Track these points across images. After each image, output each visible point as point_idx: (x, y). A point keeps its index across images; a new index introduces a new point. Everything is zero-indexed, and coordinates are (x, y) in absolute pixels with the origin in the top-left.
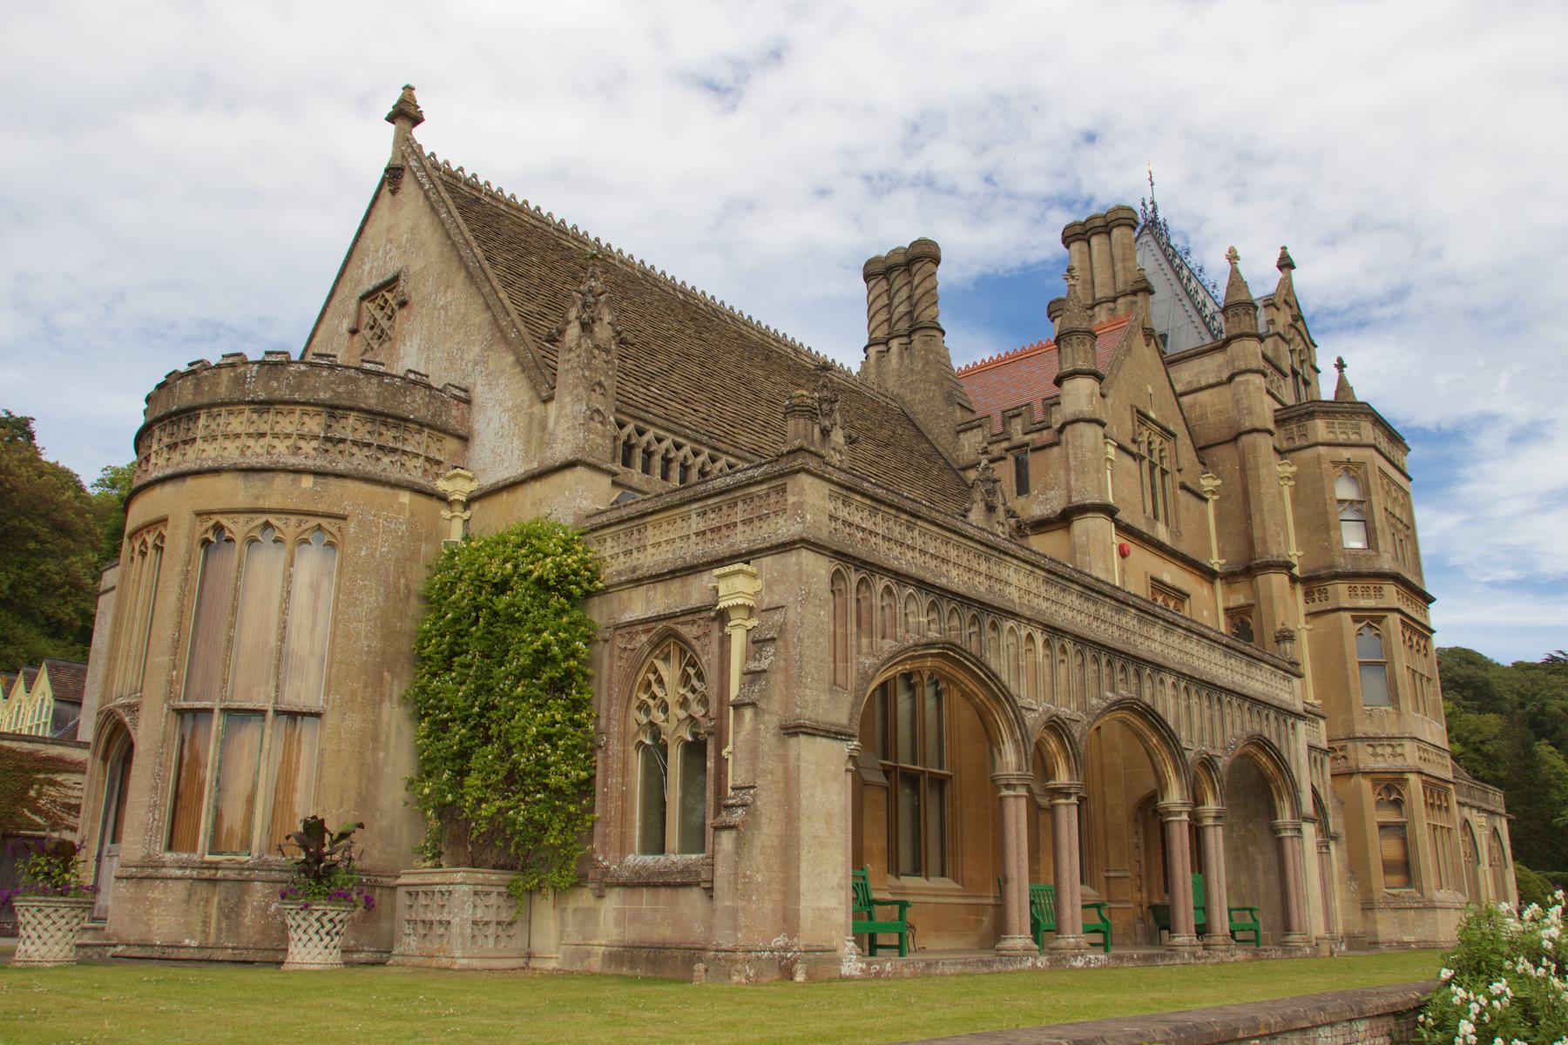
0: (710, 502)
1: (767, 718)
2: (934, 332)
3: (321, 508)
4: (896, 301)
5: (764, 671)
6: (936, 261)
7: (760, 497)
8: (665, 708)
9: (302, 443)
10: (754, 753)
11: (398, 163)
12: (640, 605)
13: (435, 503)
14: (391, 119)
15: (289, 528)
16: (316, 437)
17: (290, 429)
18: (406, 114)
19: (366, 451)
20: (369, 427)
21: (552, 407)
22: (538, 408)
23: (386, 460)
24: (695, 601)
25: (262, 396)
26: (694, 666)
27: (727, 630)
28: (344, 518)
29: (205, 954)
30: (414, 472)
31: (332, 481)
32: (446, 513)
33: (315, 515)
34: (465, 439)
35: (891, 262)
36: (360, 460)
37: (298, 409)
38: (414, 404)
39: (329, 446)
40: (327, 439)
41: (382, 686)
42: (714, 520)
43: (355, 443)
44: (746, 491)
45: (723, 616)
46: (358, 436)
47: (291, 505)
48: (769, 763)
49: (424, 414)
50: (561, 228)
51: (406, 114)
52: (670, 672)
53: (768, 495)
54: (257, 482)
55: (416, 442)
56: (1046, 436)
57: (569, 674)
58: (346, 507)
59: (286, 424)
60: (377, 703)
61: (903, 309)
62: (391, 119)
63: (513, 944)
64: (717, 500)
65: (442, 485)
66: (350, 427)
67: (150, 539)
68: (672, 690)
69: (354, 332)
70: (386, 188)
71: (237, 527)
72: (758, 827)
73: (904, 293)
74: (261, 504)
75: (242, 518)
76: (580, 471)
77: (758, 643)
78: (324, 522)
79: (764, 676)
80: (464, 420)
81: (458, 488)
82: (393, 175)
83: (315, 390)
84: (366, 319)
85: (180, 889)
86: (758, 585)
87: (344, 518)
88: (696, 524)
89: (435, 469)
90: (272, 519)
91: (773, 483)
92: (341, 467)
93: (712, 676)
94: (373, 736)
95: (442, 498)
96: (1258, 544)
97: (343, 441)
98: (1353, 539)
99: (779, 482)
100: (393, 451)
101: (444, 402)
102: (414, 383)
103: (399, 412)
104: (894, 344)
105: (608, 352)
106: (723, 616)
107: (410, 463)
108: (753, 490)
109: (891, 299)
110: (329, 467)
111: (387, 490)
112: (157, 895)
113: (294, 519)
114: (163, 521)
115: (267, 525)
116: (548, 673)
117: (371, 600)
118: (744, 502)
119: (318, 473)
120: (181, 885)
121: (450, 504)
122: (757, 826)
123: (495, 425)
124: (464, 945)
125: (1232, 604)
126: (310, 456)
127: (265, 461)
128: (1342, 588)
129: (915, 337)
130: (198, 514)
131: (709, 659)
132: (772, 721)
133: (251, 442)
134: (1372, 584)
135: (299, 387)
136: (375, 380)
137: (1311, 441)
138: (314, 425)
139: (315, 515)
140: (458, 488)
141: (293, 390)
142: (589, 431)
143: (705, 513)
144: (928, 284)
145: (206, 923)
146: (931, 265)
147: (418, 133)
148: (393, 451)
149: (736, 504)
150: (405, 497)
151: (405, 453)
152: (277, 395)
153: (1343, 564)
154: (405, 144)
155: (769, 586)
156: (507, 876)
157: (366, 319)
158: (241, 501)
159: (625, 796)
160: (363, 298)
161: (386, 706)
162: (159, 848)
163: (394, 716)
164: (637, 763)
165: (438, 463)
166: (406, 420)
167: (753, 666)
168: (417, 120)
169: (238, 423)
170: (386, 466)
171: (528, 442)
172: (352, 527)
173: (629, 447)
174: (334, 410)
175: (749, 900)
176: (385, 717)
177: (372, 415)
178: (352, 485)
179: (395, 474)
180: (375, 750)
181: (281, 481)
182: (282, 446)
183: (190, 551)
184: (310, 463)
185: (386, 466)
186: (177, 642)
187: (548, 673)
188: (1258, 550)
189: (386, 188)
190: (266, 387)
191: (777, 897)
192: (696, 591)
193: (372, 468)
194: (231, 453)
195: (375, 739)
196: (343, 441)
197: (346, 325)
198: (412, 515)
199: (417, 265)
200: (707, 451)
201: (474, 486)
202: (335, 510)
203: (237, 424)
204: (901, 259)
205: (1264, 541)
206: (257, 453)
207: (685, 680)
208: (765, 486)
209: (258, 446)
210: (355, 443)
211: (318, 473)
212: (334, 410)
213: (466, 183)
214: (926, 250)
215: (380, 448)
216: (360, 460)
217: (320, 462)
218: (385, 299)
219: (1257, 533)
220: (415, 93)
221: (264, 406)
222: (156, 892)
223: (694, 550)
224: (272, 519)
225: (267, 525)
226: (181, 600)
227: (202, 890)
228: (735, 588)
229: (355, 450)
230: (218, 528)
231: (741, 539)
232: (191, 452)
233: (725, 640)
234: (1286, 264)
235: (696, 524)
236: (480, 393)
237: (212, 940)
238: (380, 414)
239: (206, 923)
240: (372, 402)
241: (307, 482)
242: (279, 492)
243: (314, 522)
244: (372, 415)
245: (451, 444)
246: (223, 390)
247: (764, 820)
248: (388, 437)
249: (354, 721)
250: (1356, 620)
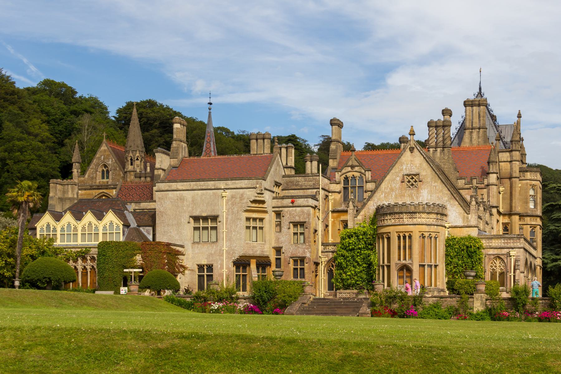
8: (496, 267)
12: (491, 252)
56: (483, 186)
86: (515, 252)
88: (503, 241)
96: (513, 207)
98: (532, 206)
125: (504, 222)
128: (528, 218)
134: (535, 218)
135: (433, 210)
137: (526, 178)
153: (530, 213)
155: (517, 253)
158: (427, 230)
169: (424, 215)
188: (513, 209)
194: (424, 221)
205: (515, 207)
219: (513, 205)
221: (428, 213)
223: (503, 245)
228: (513, 253)
230: (423, 234)
232: (415, 220)
234: (519, 116)
236: (448, 207)
241: (436, 227)
246: (421, 209)
250: (531, 227)
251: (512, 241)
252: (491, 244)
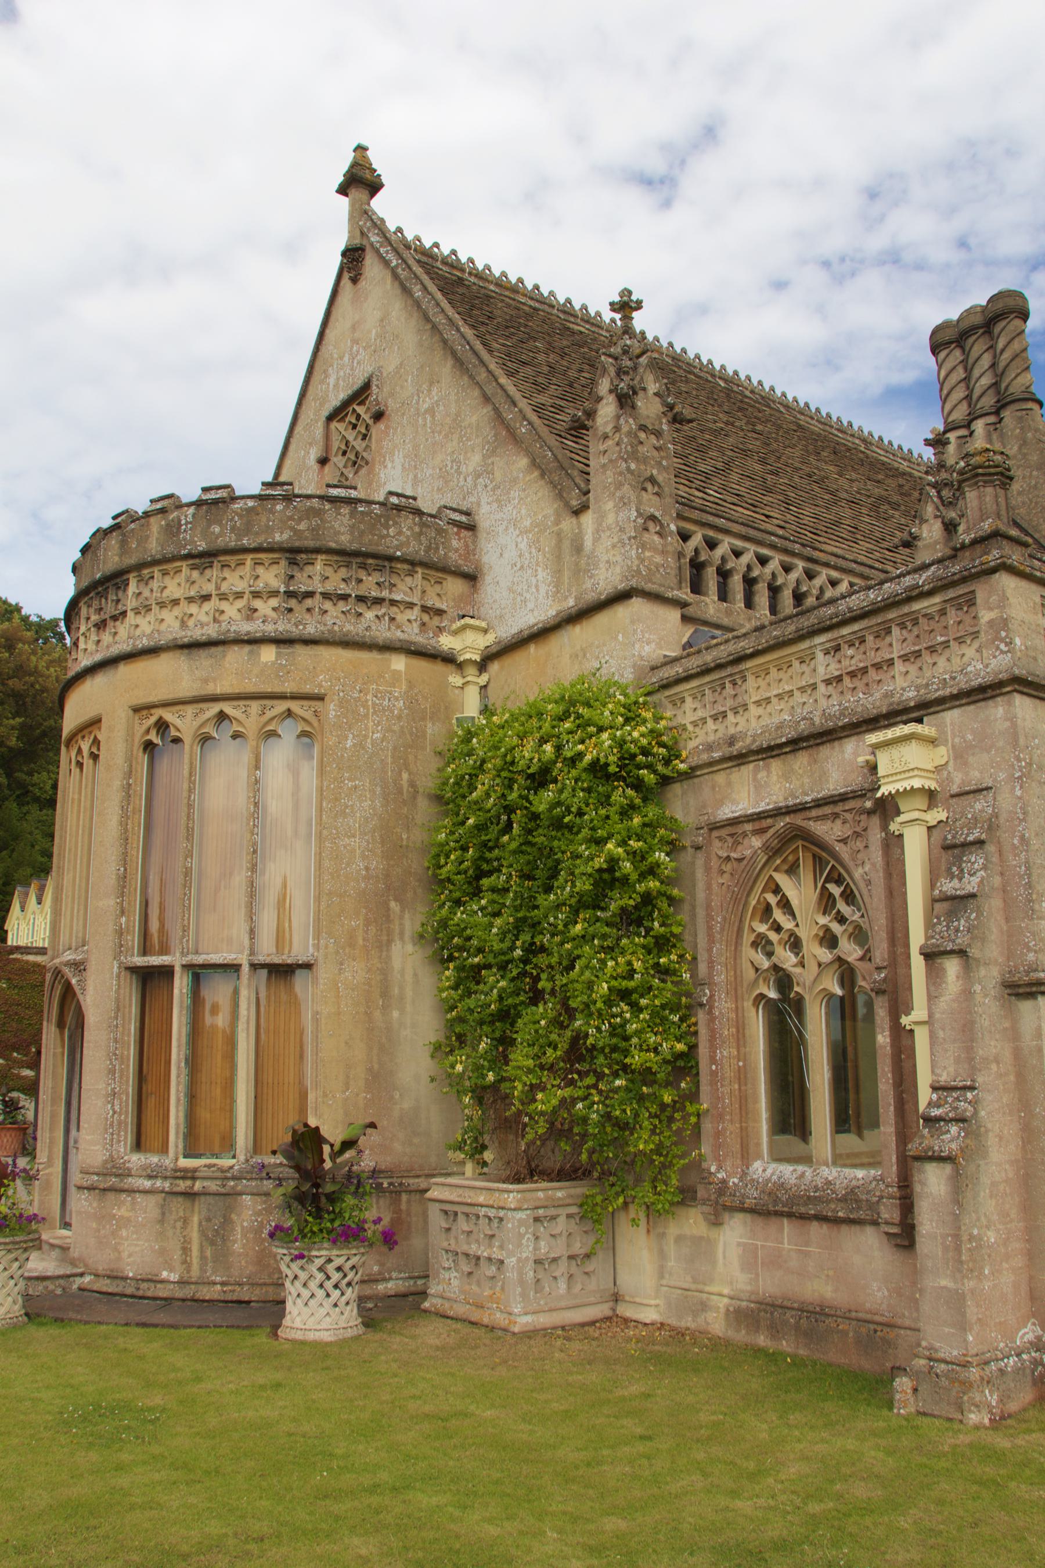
0: (845, 631)
1: (983, 972)
2: (1030, 405)
3: (288, 687)
4: (976, 373)
5: (973, 896)
6: (1024, 315)
7: (929, 617)
8: (795, 944)
9: (258, 604)
10: (967, 1030)
11: (357, 241)
12: (745, 794)
13: (439, 667)
14: (343, 190)
15: (249, 717)
16: (274, 594)
17: (240, 586)
18: (361, 181)
19: (342, 606)
20: (343, 572)
21: (588, 519)
22: (568, 524)
23: (370, 615)
24: (835, 782)
25: (202, 546)
26: (839, 881)
27: (893, 827)
28: (320, 698)
29: (188, 1292)
30: (409, 627)
31: (300, 650)
32: (456, 680)
33: (282, 697)
34: (472, 578)
35: (964, 325)
36: (335, 619)
37: (249, 558)
38: (402, 536)
39: (293, 603)
40: (290, 594)
41: (388, 919)
42: (852, 658)
43: (326, 596)
44: (906, 609)
45: (887, 808)
46: (329, 587)
47: (250, 688)
48: (992, 1045)
49: (415, 548)
50: (567, 309)
51: (361, 181)
52: (801, 891)
53: (943, 612)
54: (204, 660)
55: (408, 587)
57: (647, 899)
58: (321, 683)
59: (236, 580)
60: (383, 945)
61: (986, 381)
62: (343, 190)
63: (592, 1284)
64: (856, 627)
65: (447, 642)
66: (320, 574)
67: (85, 746)
68: (808, 919)
69: (323, 461)
70: (346, 276)
71: (185, 723)
72: (985, 1155)
73: (986, 361)
74: (211, 689)
75: (190, 710)
76: (637, 604)
77: (951, 850)
78: (295, 706)
79: (972, 904)
80: (469, 552)
81: (469, 644)
82: (353, 259)
83: (269, 530)
84: (336, 444)
85: (149, 1206)
86: (941, 755)
87: (320, 698)
88: (824, 666)
89: (436, 621)
90: (228, 708)
91: (951, 594)
92: (311, 629)
93: (876, 900)
94: (382, 990)
95: (449, 659)
97: (310, 594)
99: (961, 590)
100: (378, 601)
101: (440, 531)
102: (398, 508)
103: (381, 549)
104: (979, 426)
105: (658, 434)
106: (887, 808)
107: (402, 617)
108: (916, 606)
109: (968, 371)
110: (295, 632)
111: (375, 655)
112: (123, 1212)
113: (255, 706)
114: (96, 722)
115: (222, 716)
116: (617, 902)
117: (365, 805)
118: (902, 626)
119: (281, 641)
120: (152, 1201)
121: (460, 666)
122: (982, 1151)
123: (511, 554)
124: (524, 1295)
126: (268, 616)
127: (212, 632)
129: (1006, 413)
130: (136, 710)
131: (866, 869)
132: (989, 977)
133: (193, 609)
135: (247, 530)
136: (345, 510)
138: (271, 577)
139: (282, 697)
140: (469, 644)
141: (240, 533)
142: (643, 546)
143: (837, 649)
144: (1016, 346)
145: (186, 1250)
146: (1018, 322)
147: (379, 204)
148: (378, 601)
149: (888, 631)
150: (399, 663)
151: (393, 603)
152: (221, 543)
154: (364, 220)
155: (959, 755)
156: (578, 1189)
157: (336, 444)
158: (187, 687)
159: (743, 1076)
160: (330, 418)
161: (396, 948)
162: (123, 1147)
163: (408, 961)
164: (758, 1026)
165: (440, 612)
166: (391, 559)
167: (948, 886)
168: (374, 187)
169: (174, 585)
170: (371, 623)
171: (558, 572)
172: (331, 710)
173: (697, 566)
174: (295, 555)
175: (980, 1277)
176: (397, 963)
177: (345, 556)
178: (326, 654)
179: (383, 632)
180: (386, 1009)
181: (235, 656)
182: (232, 609)
183: (130, 759)
184: (270, 629)
185: (371, 623)
186: (123, 879)
187: (617, 902)
189: (346, 281)
190: (205, 534)
191: (1019, 1261)
192: (838, 767)
193: (351, 628)
194: (169, 625)
195: (385, 994)
196: (310, 594)
197: (314, 453)
198: (411, 685)
199: (391, 363)
200: (801, 564)
201: (489, 639)
202: (308, 688)
203: (174, 586)
204: (978, 320)
206: (202, 622)
207: (827, 903)
208: (937, 599)
209: (202, 613)
210: (326, 596)
211: (281, 641)
212: (295, 555)
213: (445, 261)
214: (1011, 302)
215: (361, 599)
216: (335, 619)
217: (283, 627)
218: (359, 410)
220: (369, 154)
221: (204, 559)
222: (122, 1208)
223: (826, 706)
224: (228, 708)
225: (222, 716)
226: (123, 824)
227: (178, 1207)
228: (906, 763)
229: (328, 605)
230: (162, 726)
231: (903, 684)
232: (123, 629)
233: (893, 844)
235: (824, 666)
236: (486, 515)
237: (195, 1273)
238: (356, 554)
239: (186, 1250)
240: (345, 540)
241: (268, 654)
242: (232, 671)
243: (281, 706)
244: (345, 556)
245: (454, 586)
246: (154, 547)
247: (992, 1141)
248: (370, 584)
249: (356, 972)
251: (897, 643)
252: (735, 724)
